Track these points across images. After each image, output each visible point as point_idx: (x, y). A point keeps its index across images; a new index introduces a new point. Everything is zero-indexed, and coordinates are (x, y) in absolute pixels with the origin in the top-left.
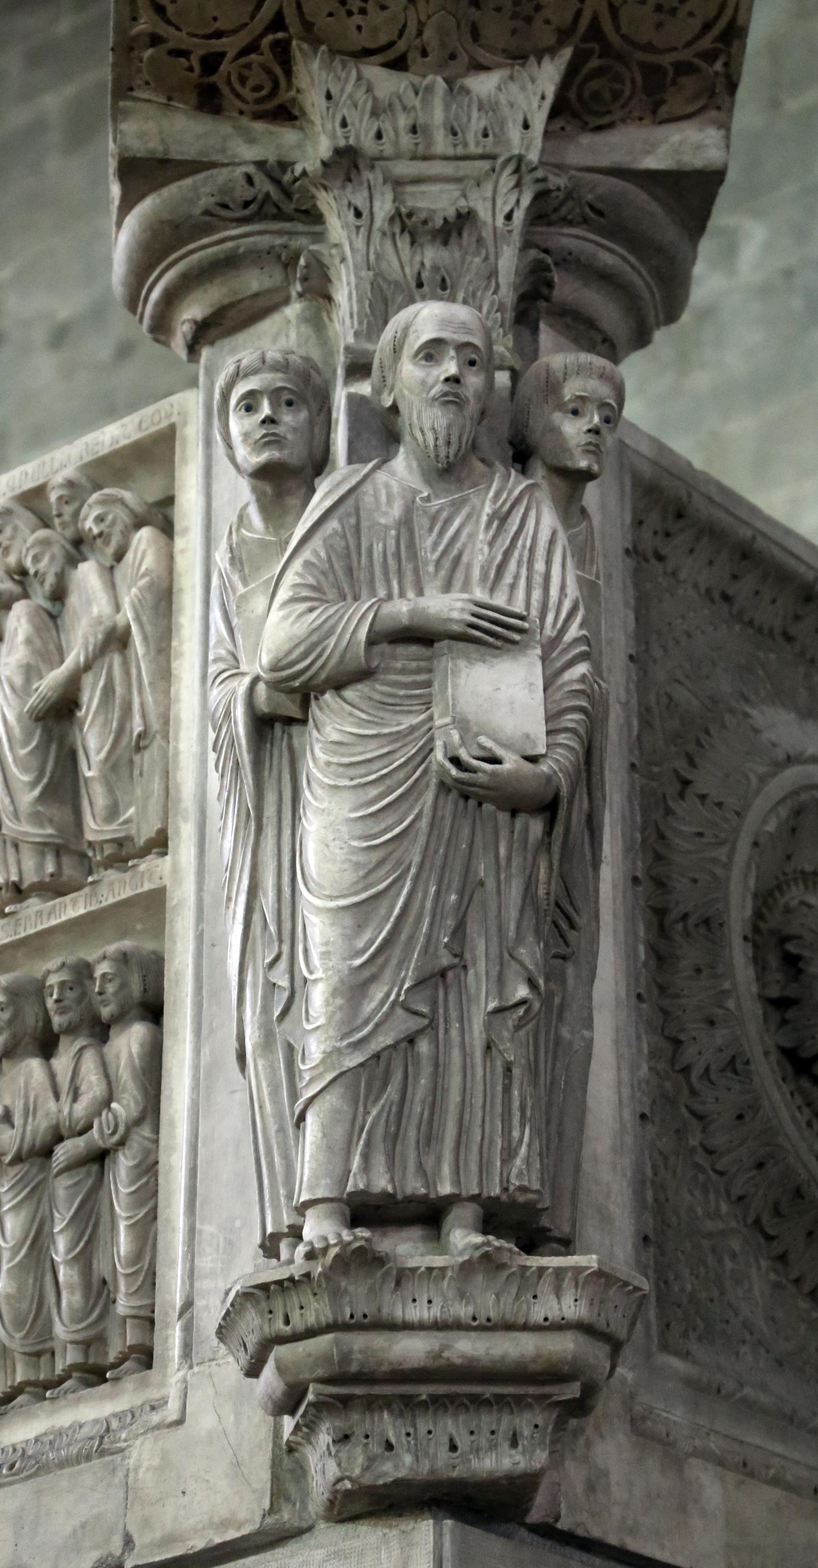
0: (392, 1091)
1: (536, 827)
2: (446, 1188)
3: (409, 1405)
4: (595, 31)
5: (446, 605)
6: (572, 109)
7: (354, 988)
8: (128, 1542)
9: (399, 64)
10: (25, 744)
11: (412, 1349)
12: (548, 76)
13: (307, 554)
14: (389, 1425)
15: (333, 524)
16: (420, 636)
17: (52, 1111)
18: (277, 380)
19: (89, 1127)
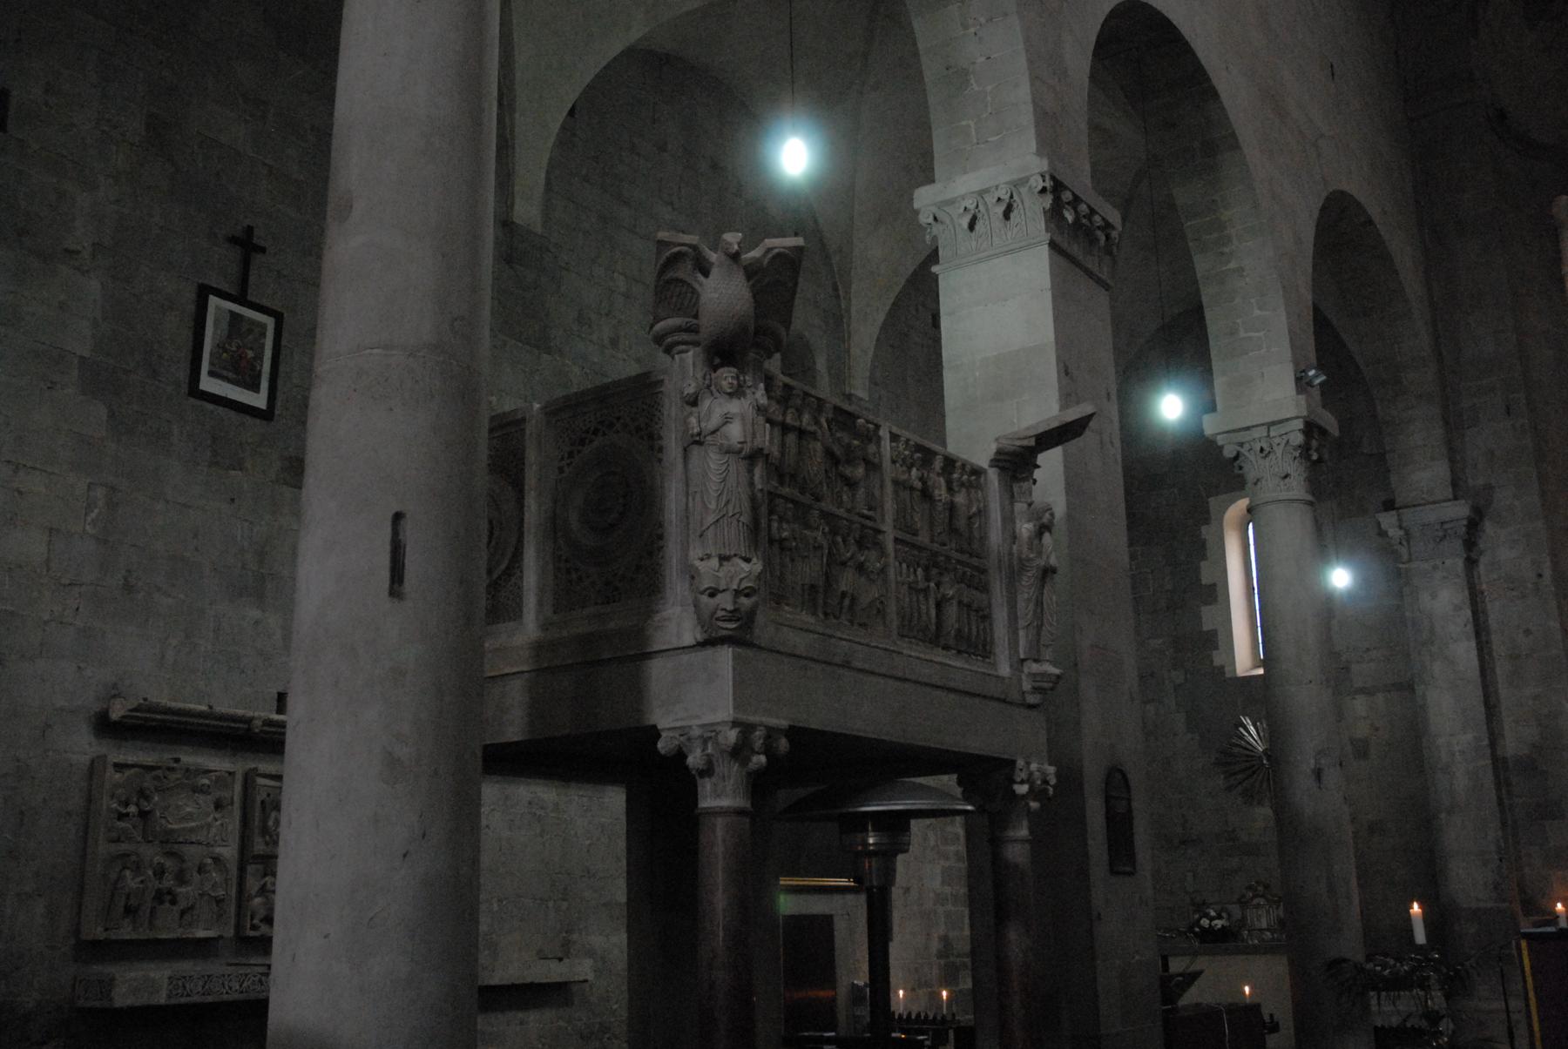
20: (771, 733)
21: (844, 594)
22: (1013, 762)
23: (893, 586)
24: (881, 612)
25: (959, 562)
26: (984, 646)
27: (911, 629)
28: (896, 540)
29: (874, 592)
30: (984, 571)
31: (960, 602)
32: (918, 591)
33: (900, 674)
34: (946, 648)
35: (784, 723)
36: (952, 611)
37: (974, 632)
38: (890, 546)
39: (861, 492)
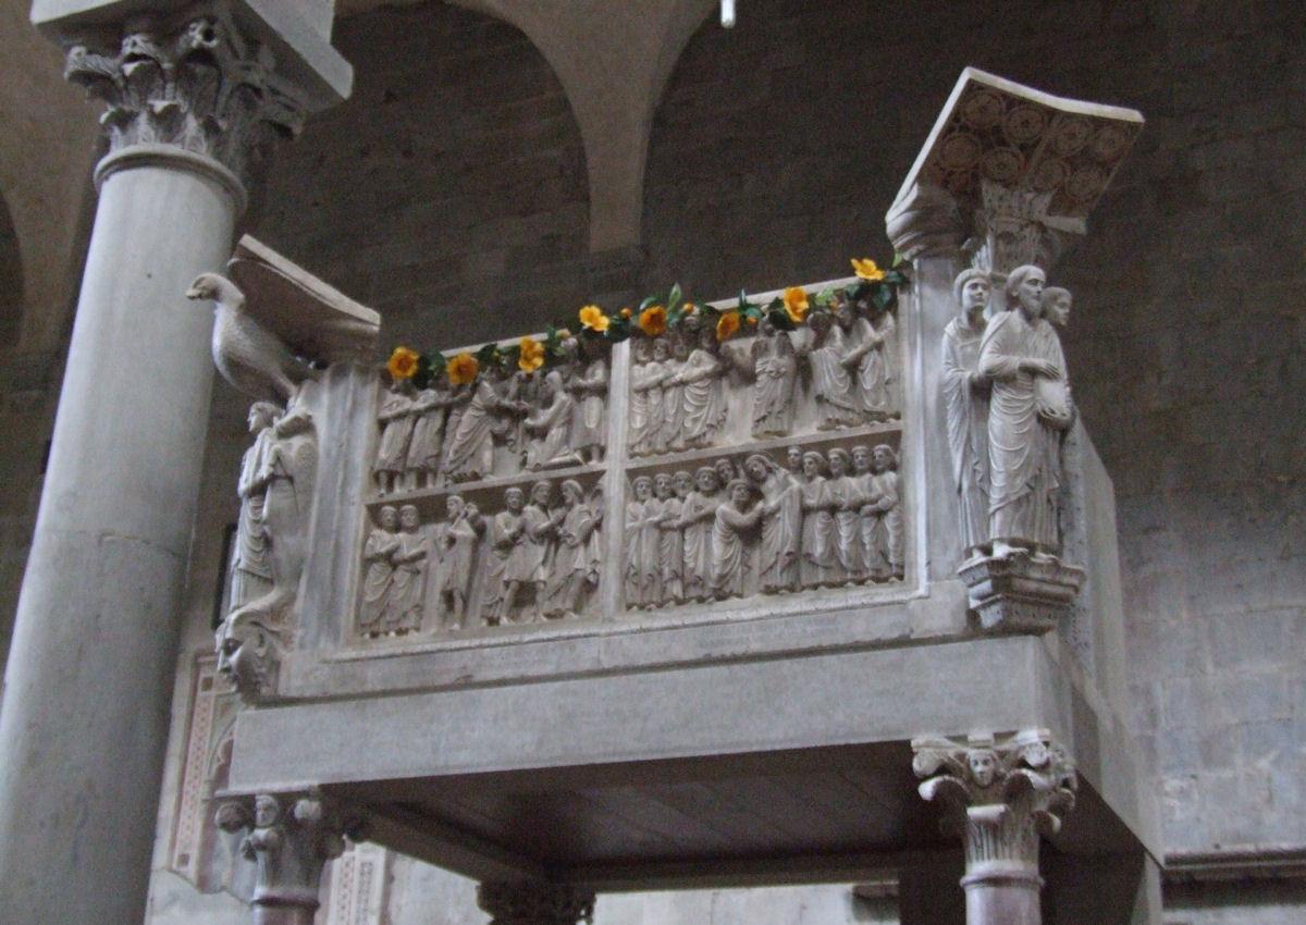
0: (1023, 510)
1: (1058, 434)
2: (1036, 540)
3: (1023, 602)
4: (1063, 189)
5: (1040, 362)
6: (1051, 211)
7: (1011, 476)
8: (912, 631)
9: (1006, 186)
10: (841, 372)
11: (1032, 586)
12: (1047, 199)
13: (994, 338)
14: (1016, 607)
15: (1002, 331)
16: (1032, 373)
17: (862, 495)
18: (983, 281)
19: (877, 502)
20: (286, 800)
21: (507, 584)
22: (904, 750)
23: (614, 541)
24: (590, 587)
25: (804, 448)
26: (884, 555)
27: (647, 591)
28: (632, 474)
29: (580, 561)
30: (895, 438)
31: (806, 511)
32: (683, 529)
33: (587, 666)
34: (770, 591)
35: (316, 783)
36: (780, 534)
37: (844, 545)
38: (614, 485)
39: (556, 433)
